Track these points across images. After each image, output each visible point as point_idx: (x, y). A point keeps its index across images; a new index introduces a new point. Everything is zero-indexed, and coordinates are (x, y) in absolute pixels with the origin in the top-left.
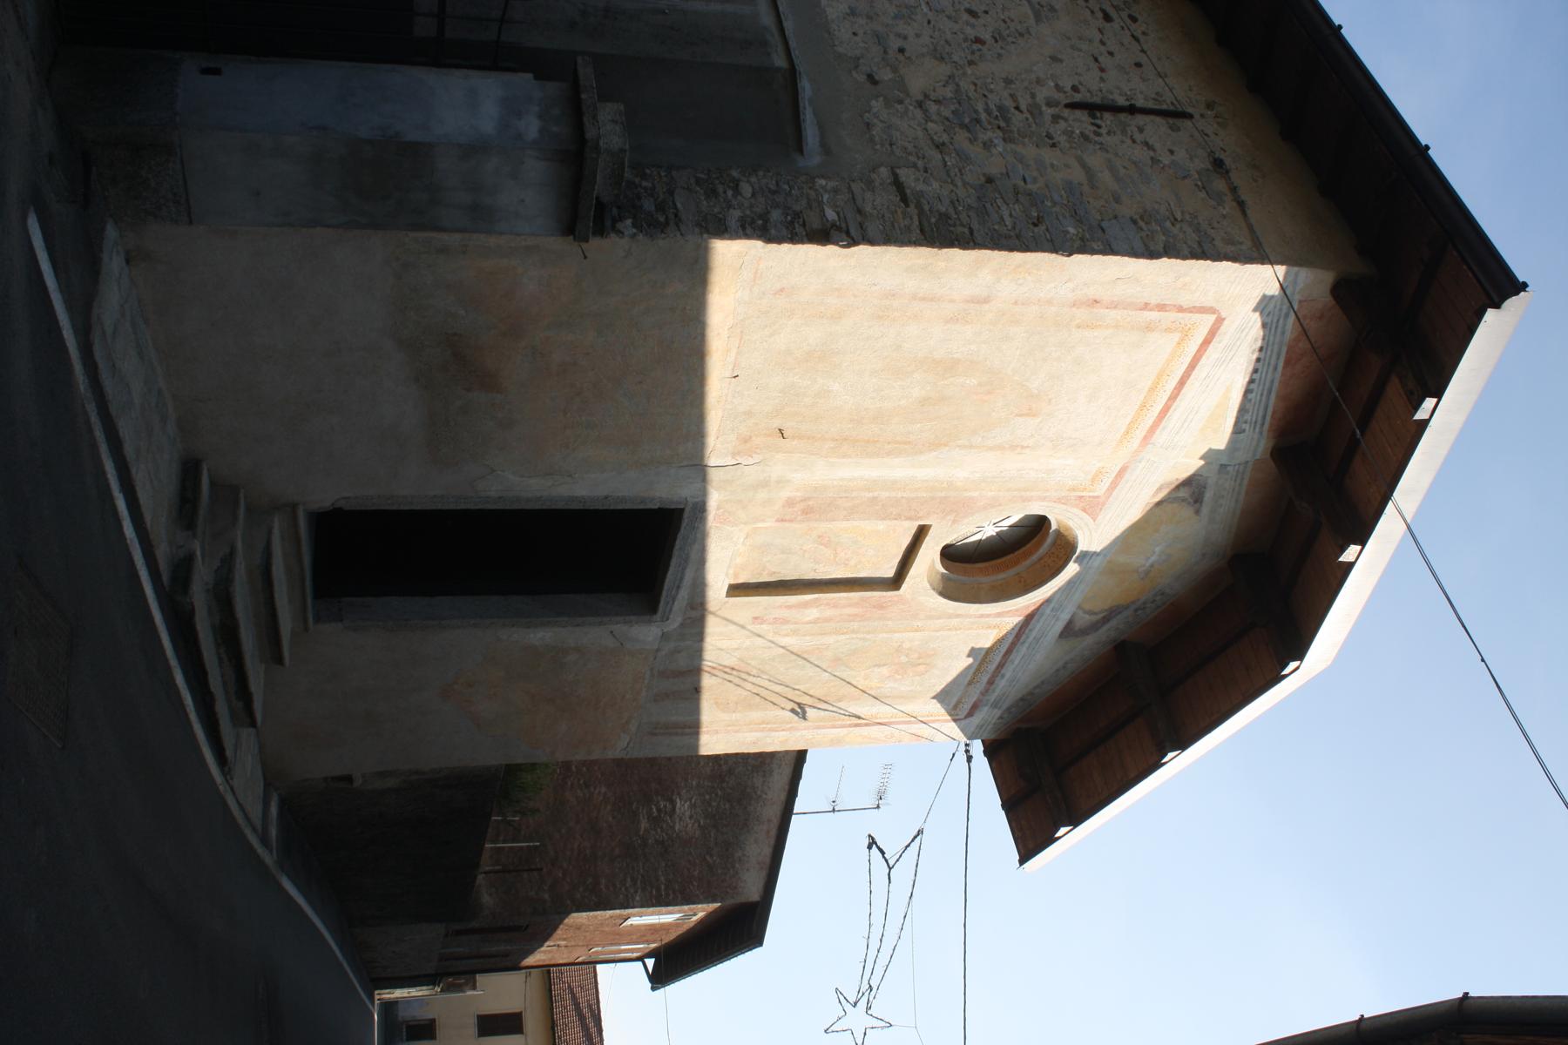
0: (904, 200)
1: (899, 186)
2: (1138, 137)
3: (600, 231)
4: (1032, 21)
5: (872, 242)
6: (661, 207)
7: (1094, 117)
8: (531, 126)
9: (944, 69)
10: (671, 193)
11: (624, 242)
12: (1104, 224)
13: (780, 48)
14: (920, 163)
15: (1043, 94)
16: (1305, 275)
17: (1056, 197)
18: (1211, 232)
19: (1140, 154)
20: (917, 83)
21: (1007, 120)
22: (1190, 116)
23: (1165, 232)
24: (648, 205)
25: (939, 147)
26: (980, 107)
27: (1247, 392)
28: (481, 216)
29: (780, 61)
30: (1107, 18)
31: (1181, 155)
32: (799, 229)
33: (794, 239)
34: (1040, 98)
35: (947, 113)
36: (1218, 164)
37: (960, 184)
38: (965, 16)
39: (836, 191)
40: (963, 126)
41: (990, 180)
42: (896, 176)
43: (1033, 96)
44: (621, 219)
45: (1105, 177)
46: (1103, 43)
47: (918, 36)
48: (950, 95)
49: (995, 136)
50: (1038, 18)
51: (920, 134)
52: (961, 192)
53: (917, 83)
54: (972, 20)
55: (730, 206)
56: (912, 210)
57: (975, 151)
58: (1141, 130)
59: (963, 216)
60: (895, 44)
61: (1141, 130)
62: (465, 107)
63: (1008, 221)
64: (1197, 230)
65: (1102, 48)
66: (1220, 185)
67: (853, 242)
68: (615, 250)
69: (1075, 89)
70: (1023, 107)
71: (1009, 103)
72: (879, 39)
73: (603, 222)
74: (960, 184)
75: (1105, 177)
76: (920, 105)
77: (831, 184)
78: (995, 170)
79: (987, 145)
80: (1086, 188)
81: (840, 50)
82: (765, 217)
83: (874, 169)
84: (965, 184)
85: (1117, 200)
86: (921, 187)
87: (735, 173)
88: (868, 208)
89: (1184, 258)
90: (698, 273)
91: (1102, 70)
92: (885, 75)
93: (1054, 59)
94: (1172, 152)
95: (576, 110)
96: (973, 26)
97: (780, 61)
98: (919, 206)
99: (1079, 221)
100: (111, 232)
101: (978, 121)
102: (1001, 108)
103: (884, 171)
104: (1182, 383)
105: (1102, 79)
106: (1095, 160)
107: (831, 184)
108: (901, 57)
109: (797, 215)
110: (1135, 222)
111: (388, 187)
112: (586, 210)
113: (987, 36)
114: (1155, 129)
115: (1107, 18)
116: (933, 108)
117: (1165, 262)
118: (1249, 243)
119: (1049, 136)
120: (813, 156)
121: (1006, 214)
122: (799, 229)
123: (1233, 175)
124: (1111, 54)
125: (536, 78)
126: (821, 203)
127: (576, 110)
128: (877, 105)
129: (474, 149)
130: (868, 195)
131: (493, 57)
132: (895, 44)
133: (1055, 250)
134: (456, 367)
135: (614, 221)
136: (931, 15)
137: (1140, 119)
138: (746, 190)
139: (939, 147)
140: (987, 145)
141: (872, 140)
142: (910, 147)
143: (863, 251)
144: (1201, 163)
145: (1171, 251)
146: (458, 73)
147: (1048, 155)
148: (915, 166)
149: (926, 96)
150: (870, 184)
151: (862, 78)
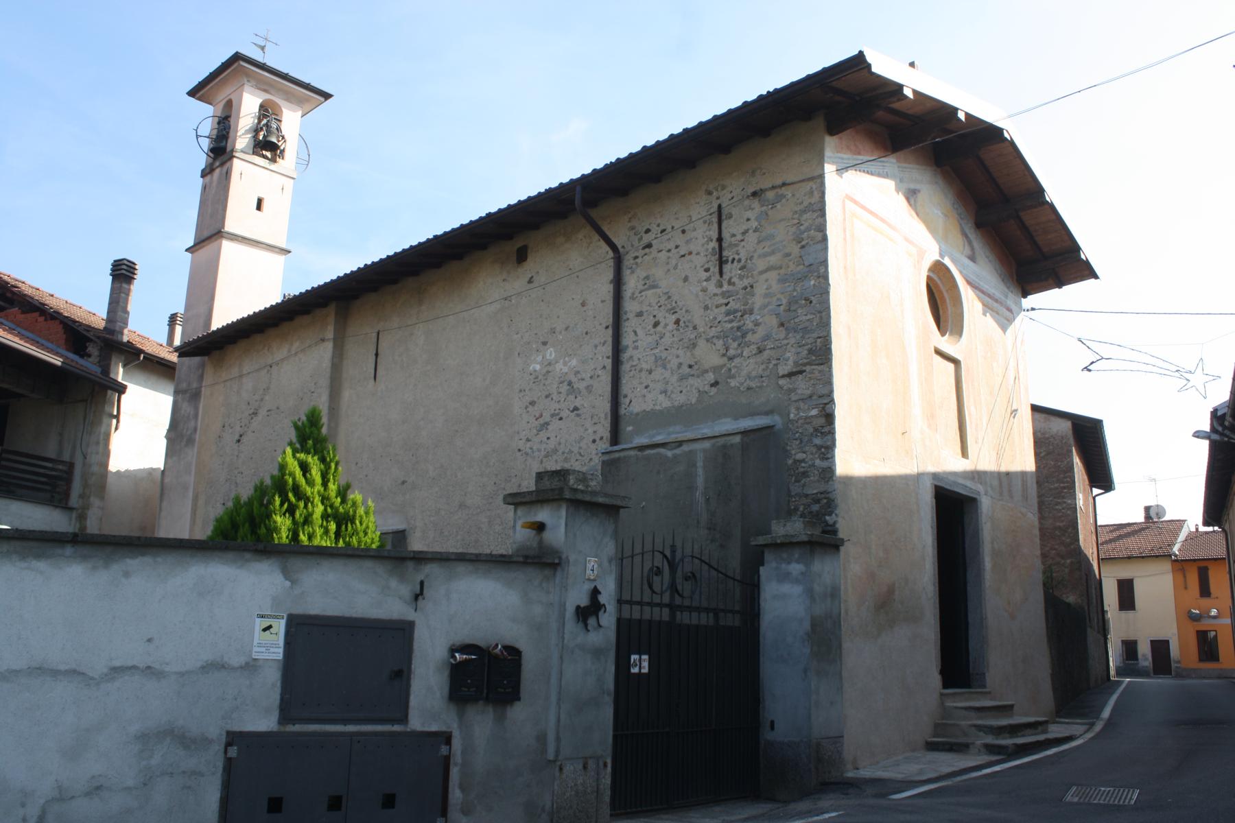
0: (801, 372)
1: (790, 375)
2: (739, 237)
3: (835, 532)
4: (658, 290)
5: (832, 391)
6: (818, 501)
7: (727, 261)
8: (796, 568)
9: (702, 343)
10: (806, 496)
11: (840, 520)
12: (807, 263)
13: (727, 438)
14: (774, 362)
15: (712, 288)
16: (828, 153)
17: (791, 289)
18: (806, 204)
19: (752, 238)
20: (715, 360)
21: (736, 311)
22: (720, 206)
23: (808, 229)
24: (816, 508)
25: (760, 351)
26: (730, 326)
27: (872, 174)
28: (834, 593)
29: (737, 439)
30: (649, 246)
31: (749, 214)
32: (826, 430)
33: (832, 433)
34: (718, 291)
35: (735, 345)
36: (754, 194)
37: (785, 342)
38: (659, 328)
39: (798, 409)
40: (743, 336)
41: (782, 325)
42: (783, 376)
43: (715, 295)
44: (826, 522)
45: (773, 260)
46: (669, 251)
47: (678, 357)
48: (721, 342)
49: (748, 321)
50: (654, 287)
51: (751, 360)
52: (792, 341)
53: (715, 360)
54: (662, 324)
55: (813, 465)
56: (808, 368)
57: (761, 332)
58: (734, 235)
59: (809, 341)
60: (686, 370)
61: (734, 235)
62: (783, 598)
63: (809, 317)
64: (804, 211)
65: (674, 251)
66: (770, 195)
67: (832, 401)
68: (846, 523)
69: (707, 270)
70: (725, 301)
71: (723, 309)
72: (683, 378)
73: (831, 530)
74: (785, 342)
75: (773, 260)
76: (731, 359)
77: (793, 410)
78: (774, 322)
79: (757, 324)
80: (782, 271)
81: (694, 401)
82: (819, 447)
83: (781, 388)
84: (786, 338)
85: (788, 255)
86: (791, 362)
87: (790, 462)
88: (809, 392)
89: (825, 221)
90: (849, 480)
91: (690, 253)
92: (711, 377)
93: (686, 279)
94: (748, 220)
95: (785, 546)
96: (666, 325)
97: (737, 439)
98: (805, 365)
99: (804, 278)
100: (850, 774)
101: (739, 328)
102: (728, 314)
103: (781, 382)
104: (871, 213)
105: (698, 254)
106: (761, 264)
107: (793, 410)
108: (696, 367)
109: (816, 430)
110: (803, 247)
111: (824, 638)
112: (827, 542)
113: (674, 317)
114: (730, 228)
115: (649, 246)
116: (731, 352)
117: (828, 233)
118: (811, 184)
119: (745, 288)
120: (776, 420)
121: (804, 318)
122: (826, 430)
123: (763, 187)
124: (677, 247)
125: (763, 565)
126: (807, 418)
127: (785, 546)
128: (733, 383)
129: (810, 593)
130: (799, 392)
131: (752, 588)
132: (686, 370)
133: (828, 293)
134: (886, 606)
135: (827, 525)
136: (661, 348)
137: (726, 235)
138: (800, 456)
139: (760, 351)
140: (757, 324)
141: (760, 387)
142: (763, 366)
143: (837, 396)
144: (756, 204)
145: (822, 228)
146: (762, 604)
147: (760, 290)
148: (776, 365)
149: (724, 355)
150: (790, 391)
151: (714, 390)
